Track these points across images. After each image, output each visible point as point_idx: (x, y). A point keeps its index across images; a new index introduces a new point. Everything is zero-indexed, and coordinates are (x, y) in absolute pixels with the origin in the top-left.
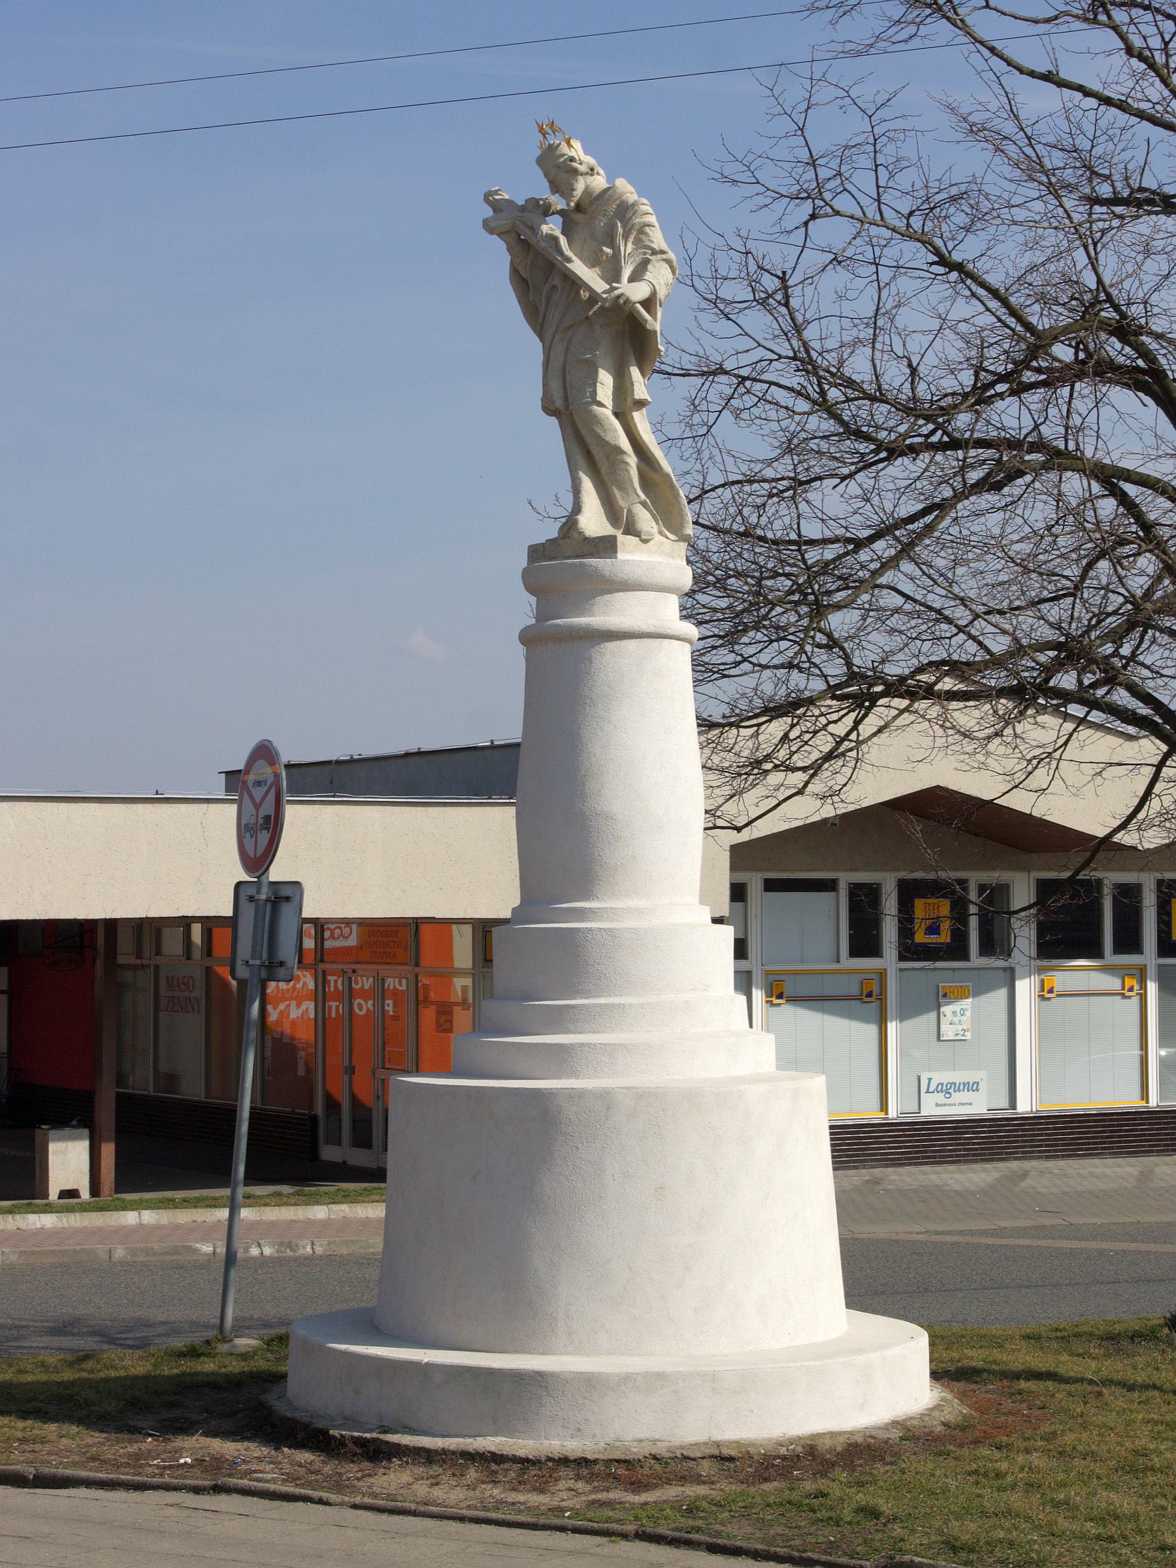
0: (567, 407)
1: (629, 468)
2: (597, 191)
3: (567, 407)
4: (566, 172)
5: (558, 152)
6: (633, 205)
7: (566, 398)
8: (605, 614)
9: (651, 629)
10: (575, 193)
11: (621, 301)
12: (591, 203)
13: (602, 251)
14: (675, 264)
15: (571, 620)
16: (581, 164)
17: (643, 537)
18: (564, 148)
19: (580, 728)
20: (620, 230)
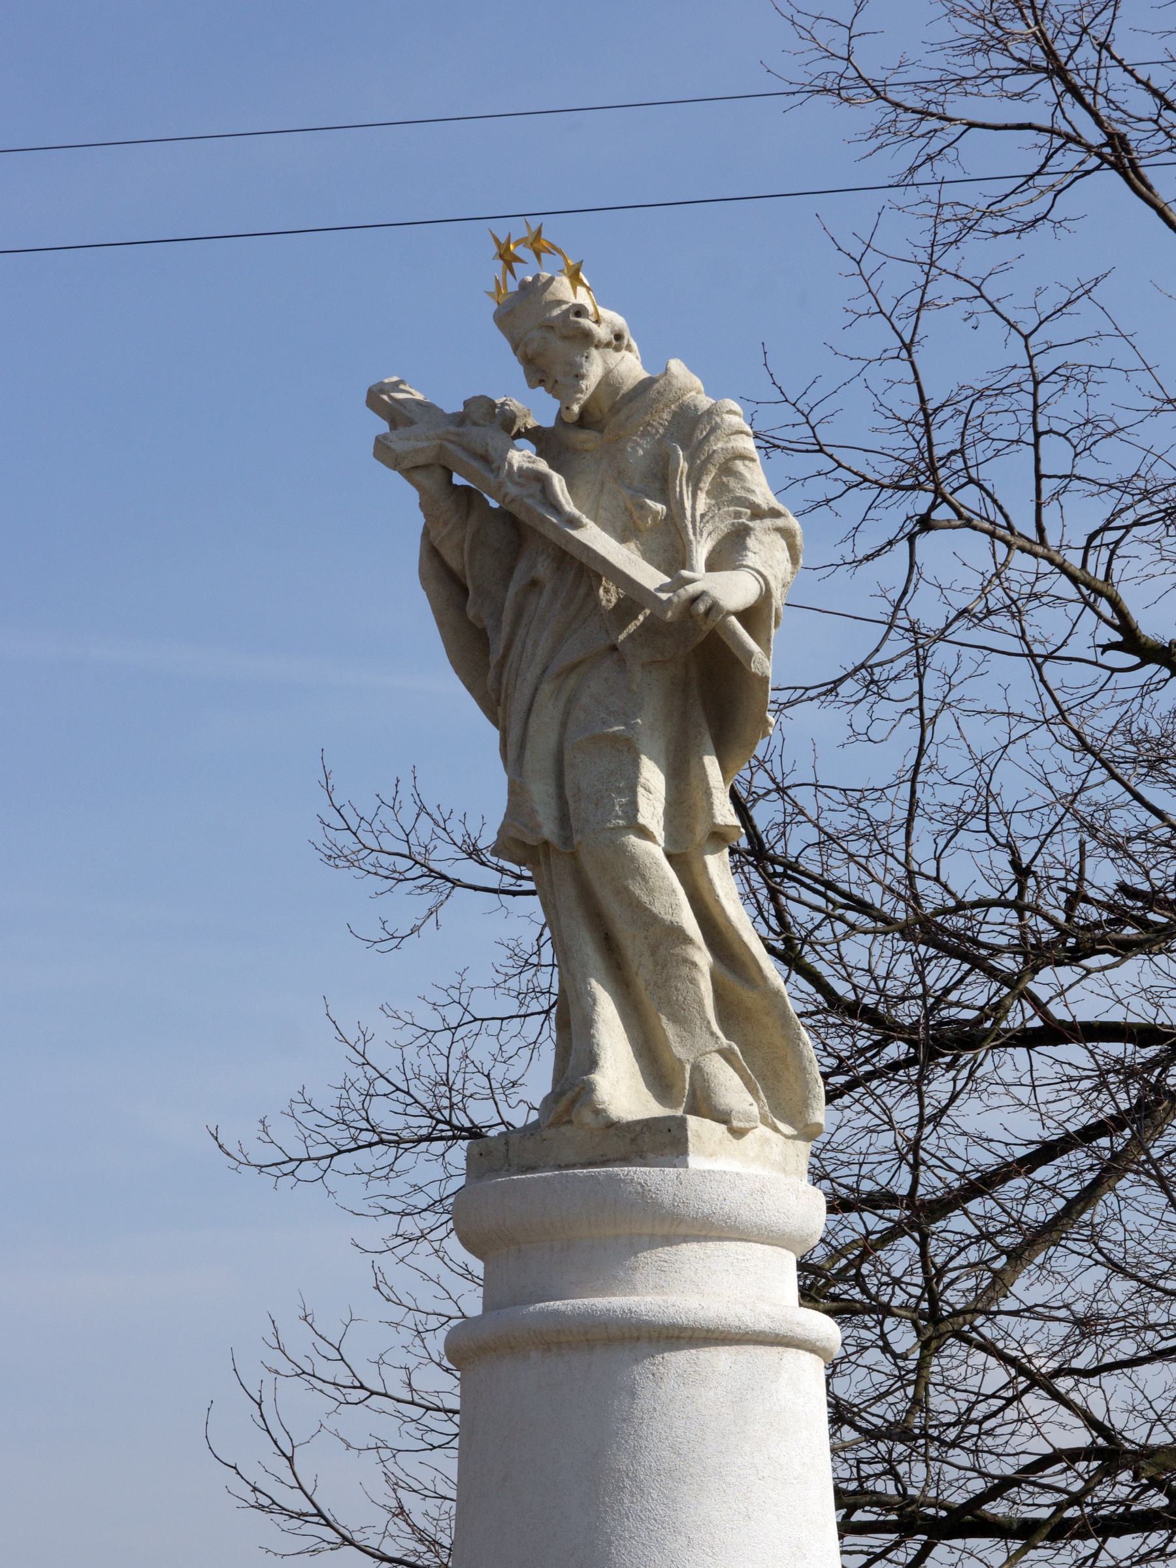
0: (567, 839)
1: (699, 977)
2: (629, 383)
3: (567, 839)
4: (565, 338)
5: (548, 297)
6: (710, 413)
7: (564, 820)
8: (658, 1288)
9: (763, 1324)
10: (583, 384)
11: (701, 607)
12: (615, 409)
13: (643, 507)
14: (799, 540)
15: (586, 1301)
16: (597, 322)
17: (736, 1124)
18: (563, 289)
19: (610, 1543)
20: (684, 465)
